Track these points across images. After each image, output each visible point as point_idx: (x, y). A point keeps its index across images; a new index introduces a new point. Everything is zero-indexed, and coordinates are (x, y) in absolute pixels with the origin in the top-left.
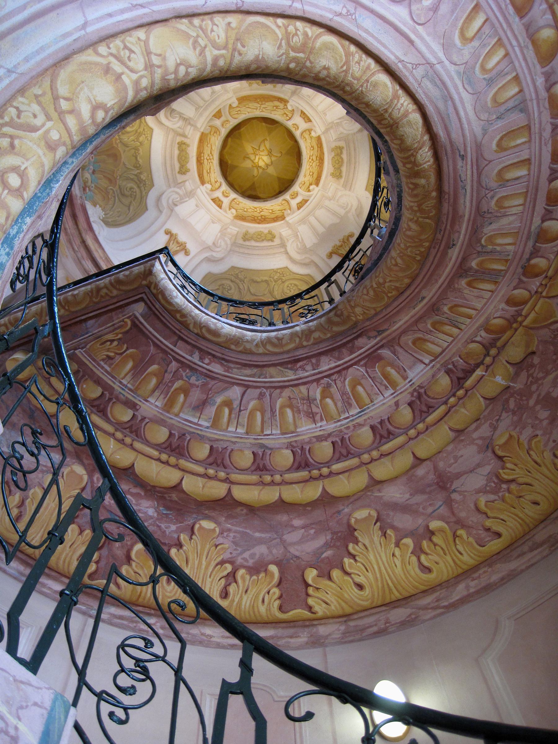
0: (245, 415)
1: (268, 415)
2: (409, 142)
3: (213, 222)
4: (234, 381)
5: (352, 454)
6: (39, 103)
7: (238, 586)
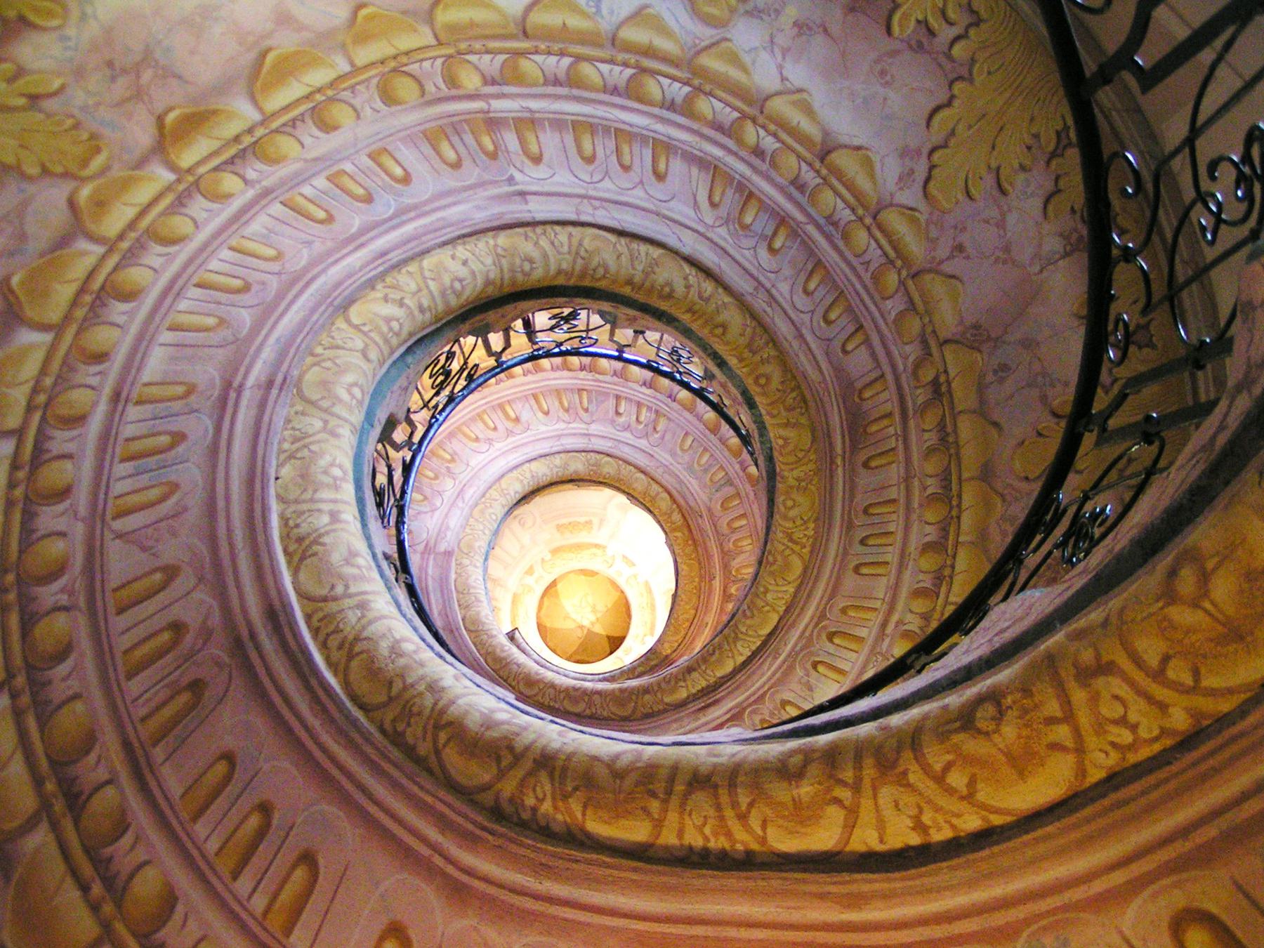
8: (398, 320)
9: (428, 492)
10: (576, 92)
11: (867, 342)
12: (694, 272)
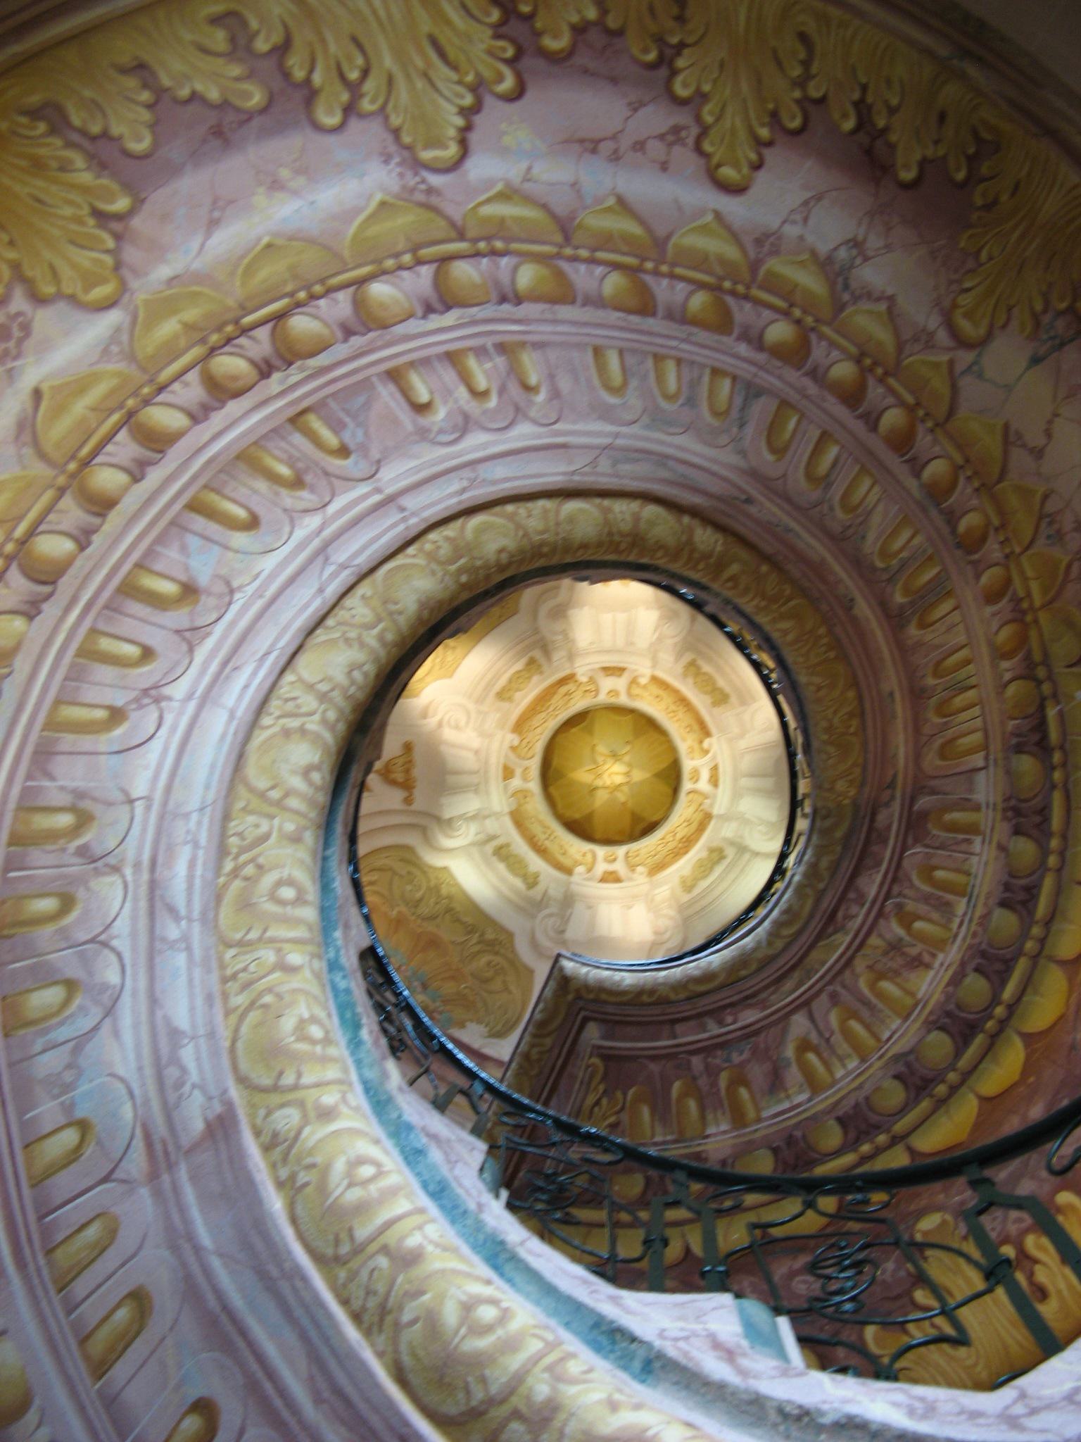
0: (837, 1039)
1: (865, 1013)
2: (671, 541)
3: (630, 907)
4: (783, 1012)
5: (1012, 959)
6: (251, 813)
7: (1044, 1264)
9: (65, 961)
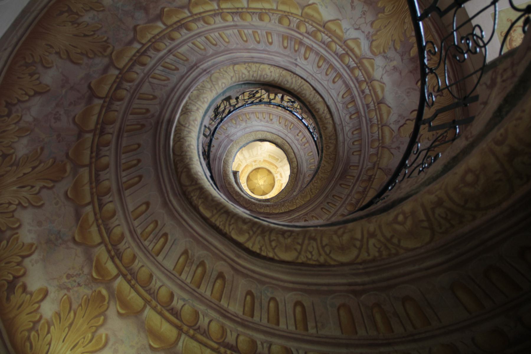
8: (245, 75)
9: (237, 122)
10: (327, 48)
11: (360, 155)
12: (327, 110)
